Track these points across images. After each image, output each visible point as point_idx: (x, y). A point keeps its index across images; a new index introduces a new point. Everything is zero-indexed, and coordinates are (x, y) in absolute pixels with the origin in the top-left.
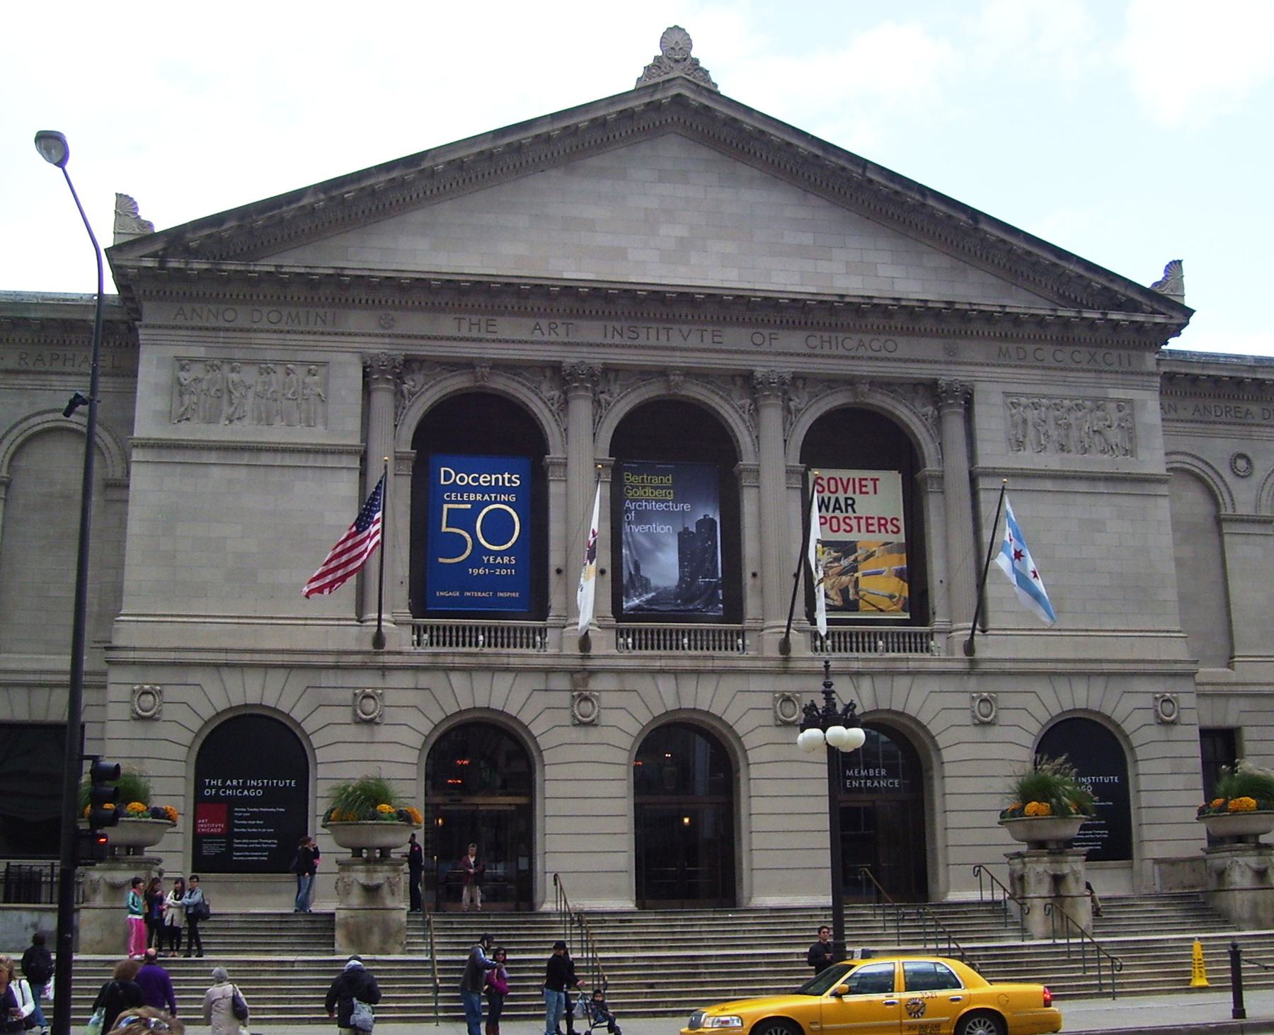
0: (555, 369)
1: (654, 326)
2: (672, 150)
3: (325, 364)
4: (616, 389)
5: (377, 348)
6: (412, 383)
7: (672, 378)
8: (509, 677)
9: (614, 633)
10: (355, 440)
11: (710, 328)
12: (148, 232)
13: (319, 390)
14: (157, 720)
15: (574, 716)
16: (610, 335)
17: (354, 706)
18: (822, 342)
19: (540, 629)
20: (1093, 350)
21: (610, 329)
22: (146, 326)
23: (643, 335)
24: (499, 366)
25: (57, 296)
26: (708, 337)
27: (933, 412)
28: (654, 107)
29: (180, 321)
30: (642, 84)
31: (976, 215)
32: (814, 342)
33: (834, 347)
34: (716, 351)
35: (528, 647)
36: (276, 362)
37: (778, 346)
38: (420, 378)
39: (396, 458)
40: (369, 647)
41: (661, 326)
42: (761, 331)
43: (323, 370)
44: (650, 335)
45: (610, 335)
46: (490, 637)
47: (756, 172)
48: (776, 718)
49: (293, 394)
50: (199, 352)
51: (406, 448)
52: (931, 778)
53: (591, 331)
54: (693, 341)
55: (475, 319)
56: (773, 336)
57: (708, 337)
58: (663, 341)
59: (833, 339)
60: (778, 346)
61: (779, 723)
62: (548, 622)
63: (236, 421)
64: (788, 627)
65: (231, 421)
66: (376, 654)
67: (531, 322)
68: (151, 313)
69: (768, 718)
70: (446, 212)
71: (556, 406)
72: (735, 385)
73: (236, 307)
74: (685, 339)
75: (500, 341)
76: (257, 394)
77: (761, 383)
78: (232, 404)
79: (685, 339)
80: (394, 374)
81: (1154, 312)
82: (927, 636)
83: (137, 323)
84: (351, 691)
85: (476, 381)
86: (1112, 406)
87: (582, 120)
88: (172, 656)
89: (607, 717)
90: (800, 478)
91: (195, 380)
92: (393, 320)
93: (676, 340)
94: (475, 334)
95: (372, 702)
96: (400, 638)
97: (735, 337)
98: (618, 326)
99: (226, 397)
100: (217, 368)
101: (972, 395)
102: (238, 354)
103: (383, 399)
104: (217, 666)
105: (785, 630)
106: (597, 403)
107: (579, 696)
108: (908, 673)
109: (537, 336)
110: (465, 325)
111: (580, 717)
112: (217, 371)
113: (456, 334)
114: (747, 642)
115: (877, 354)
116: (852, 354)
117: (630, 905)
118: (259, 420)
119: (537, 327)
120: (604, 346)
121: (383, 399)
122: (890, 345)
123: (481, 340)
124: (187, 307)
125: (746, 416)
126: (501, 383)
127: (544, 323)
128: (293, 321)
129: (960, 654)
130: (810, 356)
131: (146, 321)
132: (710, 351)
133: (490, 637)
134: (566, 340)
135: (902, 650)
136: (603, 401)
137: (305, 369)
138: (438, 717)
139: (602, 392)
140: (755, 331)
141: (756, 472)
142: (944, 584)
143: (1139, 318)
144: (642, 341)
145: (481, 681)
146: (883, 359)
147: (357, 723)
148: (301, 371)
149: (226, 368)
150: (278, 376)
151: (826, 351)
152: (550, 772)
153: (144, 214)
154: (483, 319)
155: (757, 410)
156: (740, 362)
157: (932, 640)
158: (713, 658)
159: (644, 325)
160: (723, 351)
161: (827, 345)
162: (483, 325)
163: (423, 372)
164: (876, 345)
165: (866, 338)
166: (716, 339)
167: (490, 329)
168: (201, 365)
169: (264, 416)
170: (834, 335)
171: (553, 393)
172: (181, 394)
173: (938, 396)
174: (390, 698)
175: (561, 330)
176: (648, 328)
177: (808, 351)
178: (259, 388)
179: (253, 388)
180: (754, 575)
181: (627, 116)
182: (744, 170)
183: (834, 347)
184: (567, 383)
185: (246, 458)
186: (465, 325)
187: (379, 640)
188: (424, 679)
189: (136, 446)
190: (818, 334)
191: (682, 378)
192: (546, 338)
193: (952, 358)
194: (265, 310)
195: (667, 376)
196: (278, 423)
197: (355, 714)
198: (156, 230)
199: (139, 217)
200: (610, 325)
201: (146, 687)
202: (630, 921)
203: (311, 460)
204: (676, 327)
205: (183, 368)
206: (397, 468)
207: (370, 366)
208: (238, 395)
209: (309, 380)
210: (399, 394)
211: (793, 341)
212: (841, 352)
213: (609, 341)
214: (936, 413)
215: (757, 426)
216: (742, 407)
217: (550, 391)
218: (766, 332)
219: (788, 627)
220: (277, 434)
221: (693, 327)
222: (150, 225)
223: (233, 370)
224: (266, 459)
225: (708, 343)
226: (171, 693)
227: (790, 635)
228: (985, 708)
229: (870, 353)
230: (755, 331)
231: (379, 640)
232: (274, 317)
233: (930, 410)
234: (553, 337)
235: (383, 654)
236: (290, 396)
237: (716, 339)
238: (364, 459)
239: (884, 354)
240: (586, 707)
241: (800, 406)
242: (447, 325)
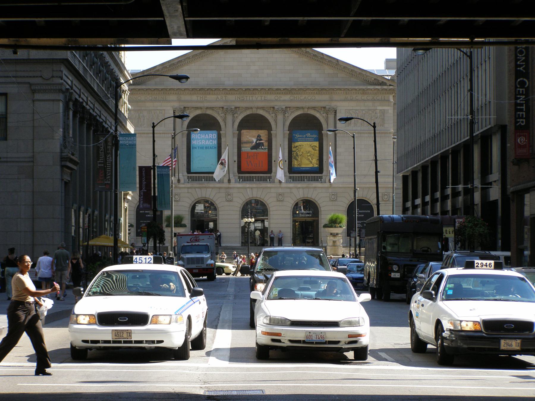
8: (211, 189)
20: (373, 96)
31: (337, 60)
41: (250, 96)
48: (277, 200)
81: (390, 85)
86: (378, 111)
92: (181, 97)
101: (336, 111)
102: (143, 108)
143: (385, 87)
148: (158, 112)
154: (204, 96)
155: (276, 117)
156: (272, 104)
162: (204, 98)
186: (199, 98)
188: (190, 190)
193: (331, 100)
204: (254, 96)
207: (175, 110)
211: (287, 97)
228: (333, 197)
240: (229, 197)
242: (194, 98)
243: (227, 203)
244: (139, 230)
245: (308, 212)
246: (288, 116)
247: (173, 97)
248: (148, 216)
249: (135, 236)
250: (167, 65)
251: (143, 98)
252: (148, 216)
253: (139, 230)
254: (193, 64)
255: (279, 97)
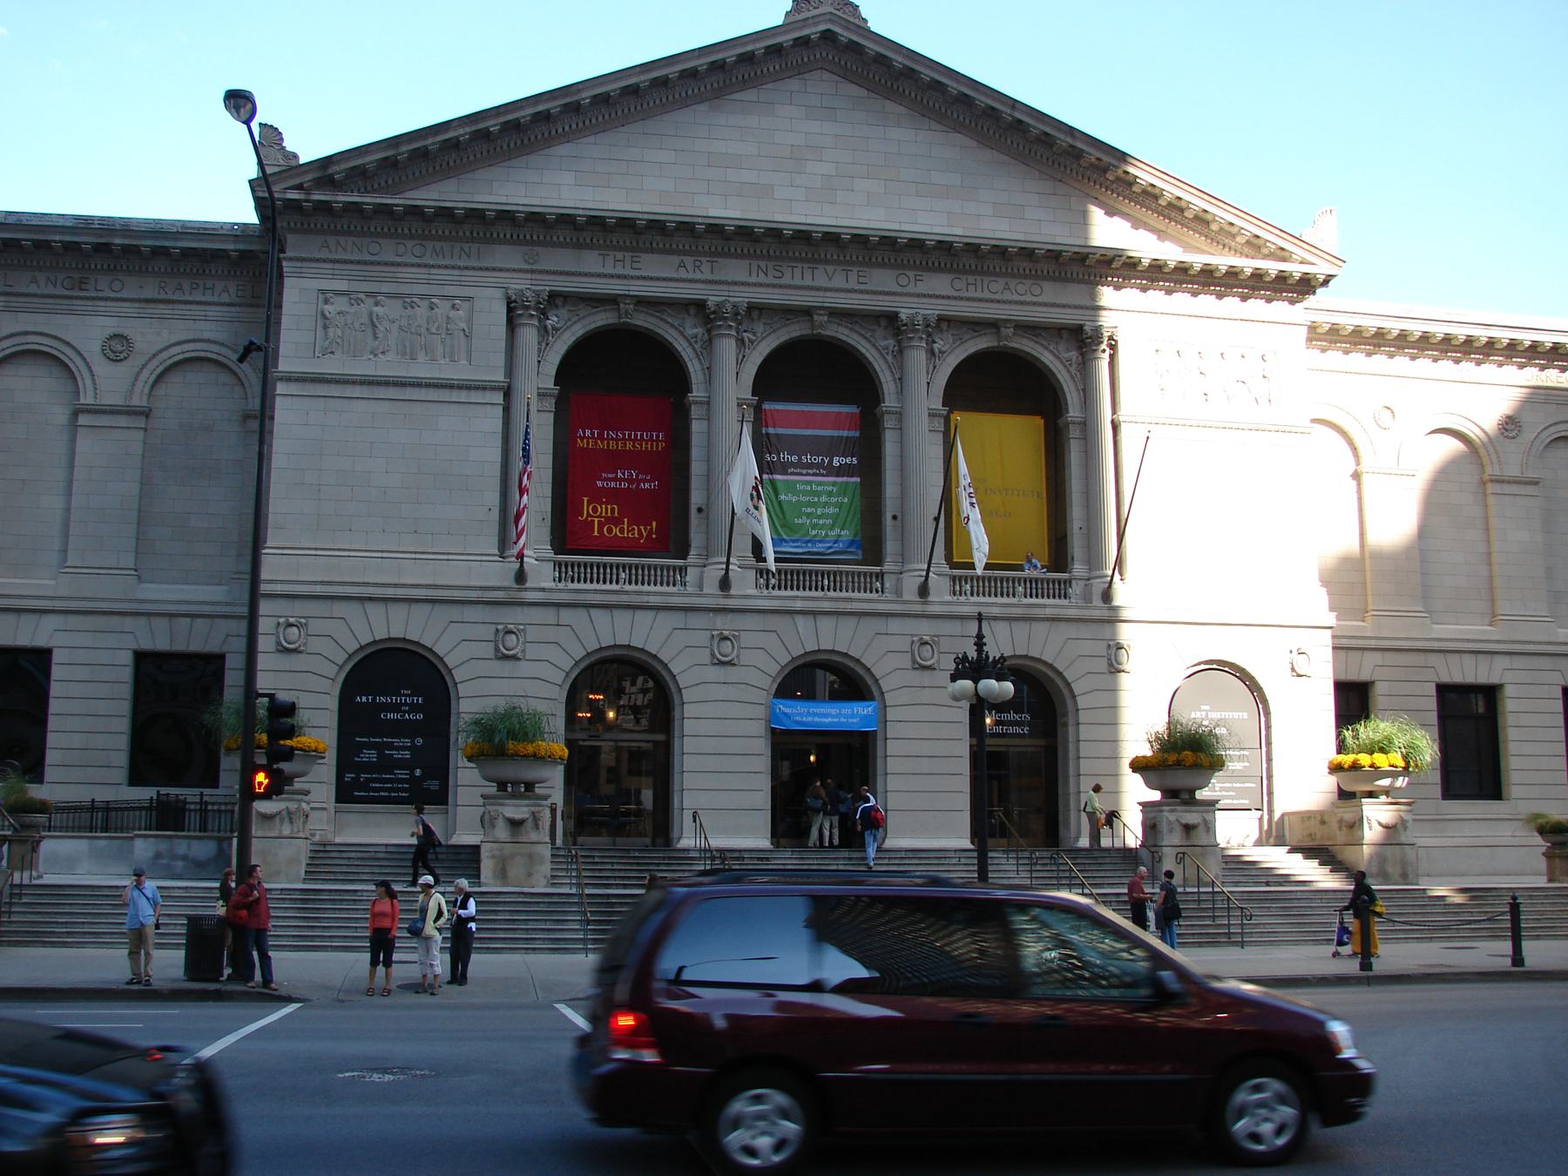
0: (700, 305)
1: (799, 265)
2: (820, 86)
3: (469, 299)
4: (760, 328)
5: (519, 284)
6: (556, 319)
7: (816, 317)
8: (650, 614)
9: (755, 571)
10: (500, 377)
11: (855, 269)
12: (293, 163)
13: (464, 325)
14: (301, 652)
15: (713, 655)
16: (754, 274)
17: (496, 642)
18: (968, 284)
19: (681, 569)
21: (754, 268)
22: (291, 259)
23: (788, 275)
24: (643, 302)
25: (198, 226)
26: (853, 277)
27: (1077, 357)
28: (803, 42)
29: (324, 254)
30: (792, 19)
32: (958, 284)
33: (979, 289)
34: (861, 292)
35: (668, 585)
36: (422, 297)
37: (922, 288)
38: (563, 312)
39: (539, 395)
40: (510, 582)
41: (806, 266)
42: (909, 273)
43: (466, 305)
44: (797, 275)
45: (754, 274)
46: (630, 574)
47: (903, 110)
48: (914, 661)
49: (438, 329)
50: (342, 285)
51: (549, 383)
52: (1065, 725)
53: (735, 270)
54: (838, 281)
55: (620, 255)
56: (918, 278)
57: (853, 277)
58: (808, 282)
59: (979, 283)
60: (922, 288)
61: (917, 666)
62: (689, 560)
63: (380, 355)
64: (928, 571)
65: (375, 355)
66: (520, 590)
67: (676, 259)
68: (295, 245)
69: (906, 661)
70: (592, 150)
71: (700, 344)
72: (880, 326)
73: (380, 241)
74: (830, 279)
75: (645, 278)
76: (400, 328)
77: (906, 325)
78: (376, 338)
79: (830, 279)
80: (537, 309)
82: (1065, 583)
83: (282, 255)
84: (494, 626)
85: (620, 318)
87: (730, 55)
88: (318, 589)
89: (747, 657)
90: (942, 421)
91: (339, 313)
93: (821, 281)
94: (619, 271)
95: (513, 636)
96: (542, 575)
97: (883, 279)
98: (763, 264)
99: (369, 331)
100: (359, 301)
103: (528, 335)
104: (361, 599)
105: (924, 573)
106: (741, 342)
107: (718, 635)
108: (1048, 619)
109: (683, 274)
110: (610, 261)
111: (720, 657)
112: (362, 305)
113: (600, 270)
114: (887, 585)
115: (1022, 298)
116: (997, 297)
117: (765, 843)
118: (404, 354)
119: (682, 265)
120: (748, 284)
121: (528, 335)
122: (1036, 290)
123: (625, 277)
124: (332, 240)
125: (889, 358)
126: (642, 320)
127: (688, 260)
128: (437, 254)
129: (1097, 601)
130: (955, 298)
131: (289, 254)
132: (855, 291)
133: (630, 574)
134: (710, 277)
135: (1040, 596)
136: (746, 340)
137: (448, 304)
138: (579, 653)
139: (745, 331)
140: (901, 272)
141: (900, 415)
142: (1084, 530)
144: (786, 280)
145: (622, 618)
146: (1028, 303)
147: (500, 659)
148: (446, 305)
149: (370, 301)
150: (422, 310)
151: (971, 294)
152: (689, 710)
153: (290, 145)
154: (628, 255)
155: (901, 351)
157: (1070, 587)
158: (850, 600)
159: (791, 264)
160: (867, 292)
161: (971, 288)
162: (628, 260)
163: (567, 308)
164: (1021, 288)
165: (1013, 283)
166: (861, 280)
167: (635, 265)
168: (345, 299)
169: (408, 350)
170: (979, 278)
171: (695, 331)
172: (325, 327)
173: (1083, 341)
174: (532, 634)
175: (706, 267)
176: (793, 267)
177: (956, 294)
178: (404, 322)
179: (397, 322)
180: (895, 517)
181: (776, 51)
182: (891, 106)
183: (979, 289)
184: (711, 321)
185: (391, 392)
187: (521, 576)
189: (281, 379)
190: (964, 277)
191: (826, 318)
192: (691, 276)
194: (410, 244)
195: (811, 316)
196: (421, 357)
197: (497, 649)
198: (302, 161)
199: (284, 148)
200: (755, 264)
201: (291, 620)
202: (767, 859)
203: (456, 396)
204: (821, 267)
205: (326, 302)
206: (540, 405)
207: (515, 301)
208: (382, 329)
209: (452, 313)
210: (544, 331)
211: (940, 283)
212: (987, 295)
213: (753, 279)
214: (1080, 358)
215: (901, 367)
216: (886, 348)
217: (694, 329)
218: (911, 274)
219: (928, 571)
220: (421, 370)
221: (839, 268)
222: (295, 156)
223: (377, 304)
224: (411, 393)
225: (853, 284)
226: (315, 626)
227: (929, 579)
229: (1016, 298)
230: (901, 272)
231: (521, 576)
232: (418, 250)
233: (1074, 354)
234: (698, 276)
235: (526, 589)
236: (434, 331)
237: (861, 280)
238: (508, 393)
239: (1029, 298)
241: (943, 349)
243: (715, 673)
244: (349, 776)
245: (1017, 717)
246: (943, 353)
247: (507, 256)
248: (390, 716)
249: (333, 800)
250: (493, 125)
251: (387, 250)
252: (390, 716)
253: (349, 776)
254: (591, 139)
255: (912, 278)
